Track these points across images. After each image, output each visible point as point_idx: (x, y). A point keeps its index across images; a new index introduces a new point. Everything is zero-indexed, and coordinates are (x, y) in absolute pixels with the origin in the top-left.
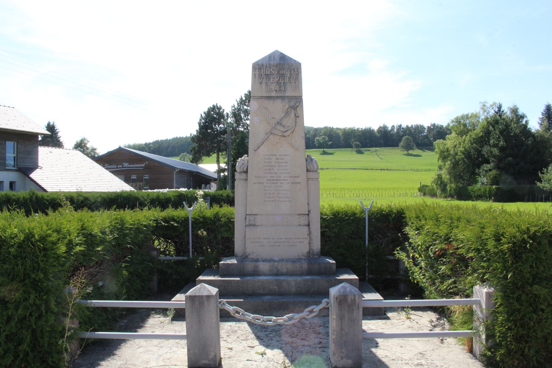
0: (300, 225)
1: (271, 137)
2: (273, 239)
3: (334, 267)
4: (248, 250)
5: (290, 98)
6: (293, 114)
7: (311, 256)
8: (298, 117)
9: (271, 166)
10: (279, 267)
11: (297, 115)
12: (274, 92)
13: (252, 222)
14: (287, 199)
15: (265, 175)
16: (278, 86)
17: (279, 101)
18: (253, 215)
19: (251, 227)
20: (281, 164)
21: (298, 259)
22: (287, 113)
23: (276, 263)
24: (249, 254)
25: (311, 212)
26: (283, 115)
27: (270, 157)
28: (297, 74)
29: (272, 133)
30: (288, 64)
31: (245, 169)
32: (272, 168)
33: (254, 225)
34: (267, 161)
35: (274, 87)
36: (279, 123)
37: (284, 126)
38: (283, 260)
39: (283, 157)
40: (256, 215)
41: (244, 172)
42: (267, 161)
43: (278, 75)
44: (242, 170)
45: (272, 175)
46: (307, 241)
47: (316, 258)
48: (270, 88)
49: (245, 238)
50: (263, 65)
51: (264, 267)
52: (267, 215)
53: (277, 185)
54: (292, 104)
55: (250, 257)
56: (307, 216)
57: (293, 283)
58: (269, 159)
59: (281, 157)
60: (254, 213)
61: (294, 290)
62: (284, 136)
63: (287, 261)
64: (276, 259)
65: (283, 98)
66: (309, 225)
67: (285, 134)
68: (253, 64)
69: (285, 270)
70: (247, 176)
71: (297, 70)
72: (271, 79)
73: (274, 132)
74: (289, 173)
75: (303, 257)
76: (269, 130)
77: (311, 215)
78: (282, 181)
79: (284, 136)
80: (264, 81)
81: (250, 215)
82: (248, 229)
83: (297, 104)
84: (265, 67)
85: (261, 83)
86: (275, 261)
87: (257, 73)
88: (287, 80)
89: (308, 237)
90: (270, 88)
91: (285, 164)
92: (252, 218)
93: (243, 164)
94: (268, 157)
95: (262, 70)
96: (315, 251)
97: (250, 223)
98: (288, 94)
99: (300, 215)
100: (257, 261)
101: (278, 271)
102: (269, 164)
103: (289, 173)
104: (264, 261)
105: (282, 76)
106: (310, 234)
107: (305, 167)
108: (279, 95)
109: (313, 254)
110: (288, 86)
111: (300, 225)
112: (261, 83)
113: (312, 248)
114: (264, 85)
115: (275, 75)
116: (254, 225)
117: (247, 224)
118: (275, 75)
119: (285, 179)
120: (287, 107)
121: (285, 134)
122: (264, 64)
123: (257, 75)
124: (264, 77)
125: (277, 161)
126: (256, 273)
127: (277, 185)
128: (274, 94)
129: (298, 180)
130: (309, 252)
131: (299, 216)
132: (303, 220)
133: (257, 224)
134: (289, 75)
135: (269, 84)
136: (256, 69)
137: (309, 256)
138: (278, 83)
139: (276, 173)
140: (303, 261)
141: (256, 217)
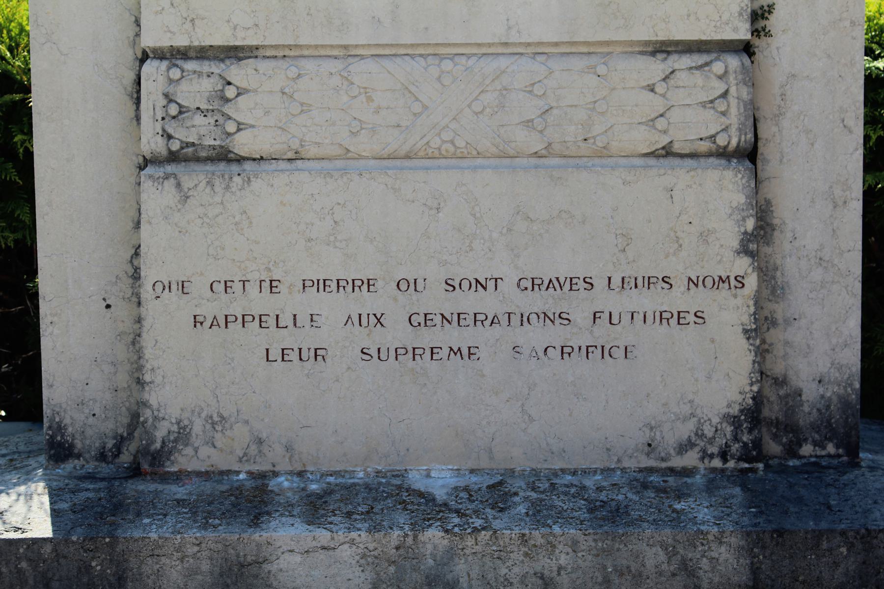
0: (668, 152)
2: (408, 285)
4: (173, 398)
7: (773, 448)
13: (199, 131)
18: (203, 53)
19: (194, 177)
21: (641, 481)
23: (434, 537)
24: (183, 435)
25: (774, 22)
33: (224, 156)
38: (498, 495)
40: (234, 53)
46: (731, 313)
47: (815, 467)
49: (136, 276)
55: (184, 460)
56: (734, 62)
60: (218, 39)
63: (539, 514)
64: (440, 481)
66: (750, 154)
75: (691, 459)
77: (784, 49)
81: (175, 55)
82: (157, 197)
86: (426, 508)
89: (742, 265)
92: (196, 88)
96: (811, 392)
97: (182, 134)
99: (662, 49)
100: (251, 501)
104: (316, 507)
106: (760, 232)
109: (790, 431)
111: (668, 152)
113: (777, 368)
116: (224, 156)
117: (151, 141)
130: (752, 415)
131: (656, 68)
132: (699, 104)
133: (243, 144)
137: (753, 453)
140: (702, 512)
141: (239, 73)
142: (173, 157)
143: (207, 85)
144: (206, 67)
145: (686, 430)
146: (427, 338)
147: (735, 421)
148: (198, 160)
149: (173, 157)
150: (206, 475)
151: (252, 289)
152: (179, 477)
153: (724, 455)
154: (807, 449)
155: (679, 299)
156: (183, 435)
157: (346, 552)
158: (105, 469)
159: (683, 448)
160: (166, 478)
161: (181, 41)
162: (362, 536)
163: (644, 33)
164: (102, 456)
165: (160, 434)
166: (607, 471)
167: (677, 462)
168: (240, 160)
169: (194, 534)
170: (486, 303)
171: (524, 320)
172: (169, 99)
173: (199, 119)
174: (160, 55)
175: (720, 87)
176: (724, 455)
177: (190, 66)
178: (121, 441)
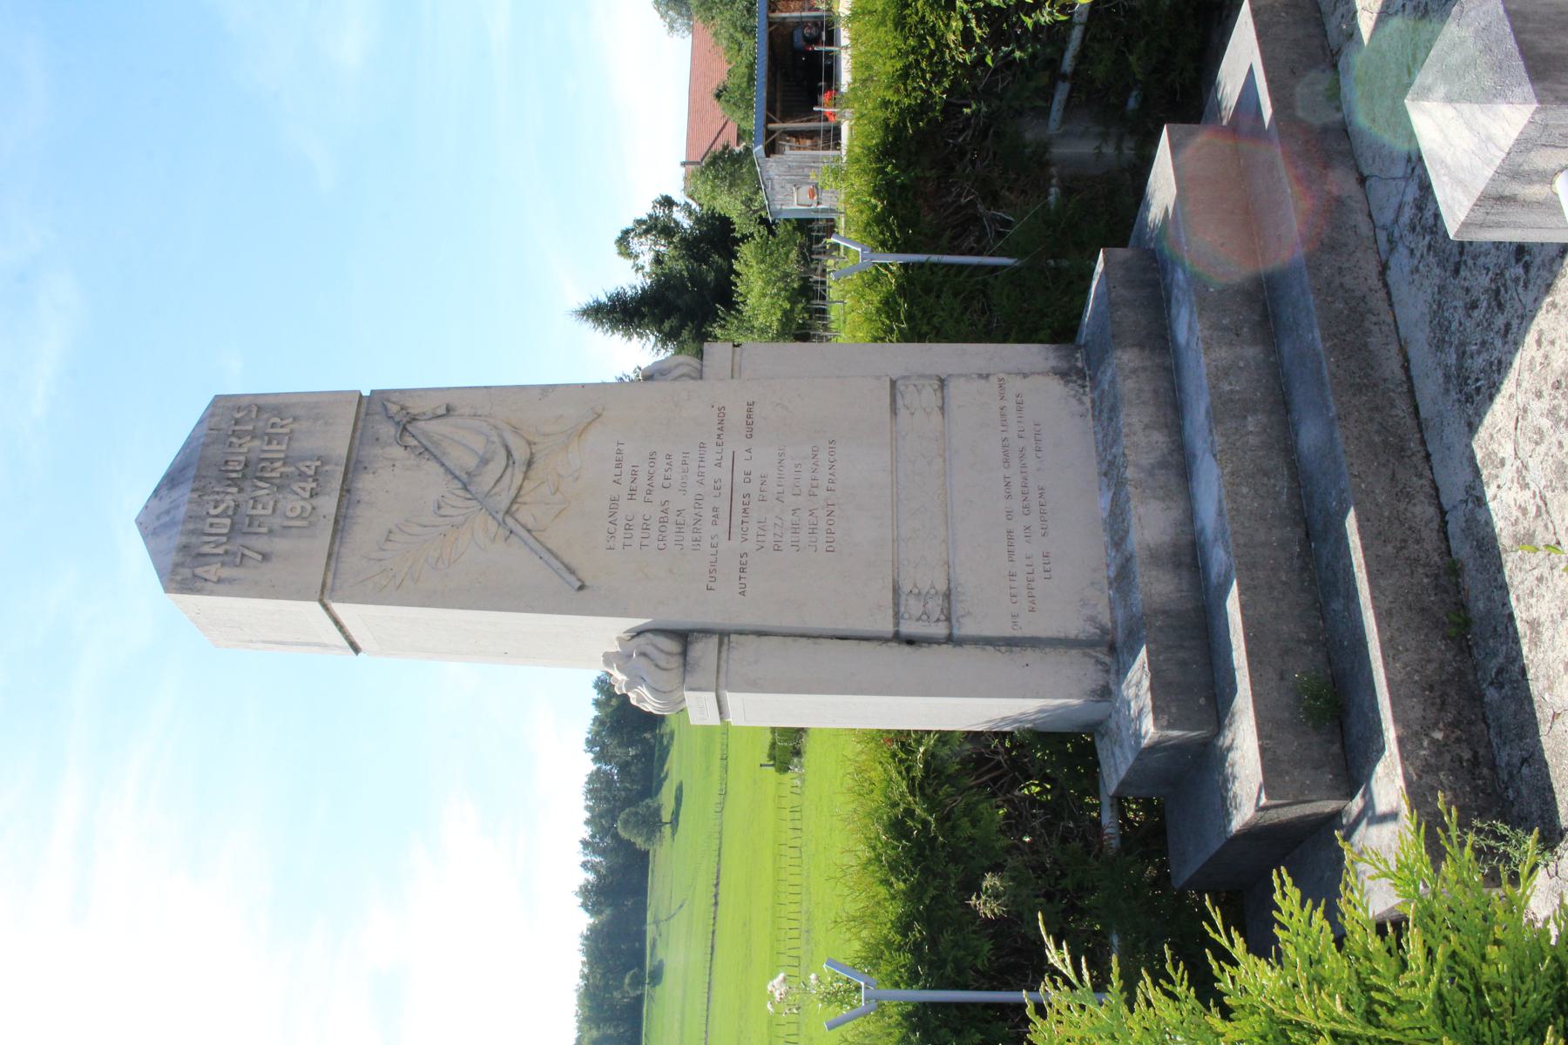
0: (942, 408)
1: (524, 515)
2: (1009, 514)
3: (1120, 253)
5: (360, 433)
6: (434, 427)
8: (448, 409)
9: (663, 522)
10: (1147, 460)
11: (442, 411)
12: (317, 501)
13: (935, 606)
14: (823, 456)
15: (705, 545)
16: (295, 487)
17: (366, 483)
18: (896, 604)
19: (958, 609)
20: (658, 480)
22: (427, 451)
24: (1092, 619)
26: (432, 466)
27: (621, 522)
28: (260, 409)
29: (508, 512)
30: (205, 445)
31: (672, 646)
32: (672, 517)
33: (948, 596)
34: (637, 533)
35: (293, 504)
36: (465, 482)
37: (484, 461)
39: (627, 468)
40: (896, 590)
41: (684, 653)
42: (637, 533)
43: (247, 484)
44: (675, 662)
45: (708, 514)
48: (299, 517)
50: (185, 548)
51: (1151, 524)
52: (896, 540)
53: (755, 495)
54: (388, 430)
57: (1223, 354)
58: (628, 528)
59: (626, 479)
60: (890, 595)
61: (1252, 352)
62: (530, 464)
64: (1103, 503)
65: (353, 467)
67: (520, 453)
68: (167, 590)
69: (1159, 438)
70: (706, 632)
71: (239, 409)
72: (259, 511)
73: (504, 501)
74: (702, 446)
75: (1087, 400)
76: (492, 526)
78: (739, 477)
79: (530, 464)
80: (261, 543)
81: (897, 616)
83: (394, 409)
84: (194, 540)
85: (265, 557)
87: (213, 571)
88: (277, 450)
90: (299, 517)
91: (661, 462)
92: (912, 606)
93: (643, 654)
94: (620, 533)
95: (206, 549)
97: (937, 613)
98: (338, 445)
99: (894, 411)
101: (1163, 464)
102: (655, 527)
103: (702, 446)
105: (252, 471)
107: (677, 384)
108: (336, 484)
110: (305, 445)
111: (942, 408)
112: (265, 557)
114: (280, 545)
115: (241, 498)
116: (948, 596)
118: (241, 498)
119: (727, 463)
120: (397, 452)
121: (520, 453)
122: (180, 540)
123: (226, 572)
124: (240, 540)
125: (640, 496)
126: (1189, 556)
127: (755, 495)
128: (328, 504)
129: (736, 416)
131: (902, 412)
133: (942, 586)
134: (257, 443)
135: (277, 522)
136: (195, 576)
138: (281, 486)
139: (699, 499)
141: (906, 587)
142: (948, 619)
143: (912, 601)
144: (903, 602)
145: (1074, 402)
146: (1035, 507)
147: (1067, 382)
148: (949, 609)
149: (948, 619)
150: (1112, 609)
151: (1014, 584)
152: (1114, 622)
153: (1084, 387)
154: (1079, 364)
155: (1011, 404)
156: (1092, 619)
157: (1141, 510)
158: (1113, 670)
159: (1081, 402)
160: (1115, 628)
161: (891, 612)
162: (1133, 503)
163: (888, 415)
164: (1107, 671)
165: (1092, 630)
166: (1095, 433)
167: (1089, 405)
168: (949, 589)
169: (1139, 580)
170: (1016, 482)
171: (1024, 466)
172: (919, 619)
173: (929, 606)
174: (897, 624)
175: (911, 388)
176: (1084, 387)
177: (902, 609)
178: (1098, 662)
